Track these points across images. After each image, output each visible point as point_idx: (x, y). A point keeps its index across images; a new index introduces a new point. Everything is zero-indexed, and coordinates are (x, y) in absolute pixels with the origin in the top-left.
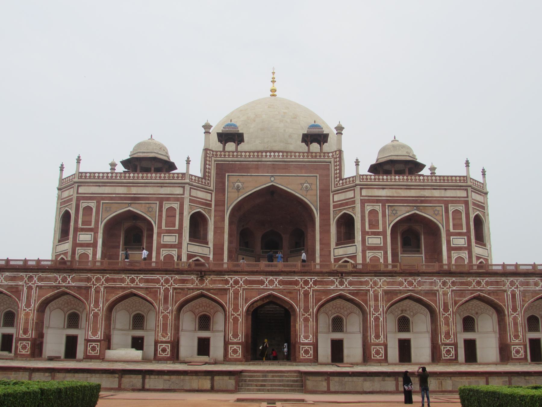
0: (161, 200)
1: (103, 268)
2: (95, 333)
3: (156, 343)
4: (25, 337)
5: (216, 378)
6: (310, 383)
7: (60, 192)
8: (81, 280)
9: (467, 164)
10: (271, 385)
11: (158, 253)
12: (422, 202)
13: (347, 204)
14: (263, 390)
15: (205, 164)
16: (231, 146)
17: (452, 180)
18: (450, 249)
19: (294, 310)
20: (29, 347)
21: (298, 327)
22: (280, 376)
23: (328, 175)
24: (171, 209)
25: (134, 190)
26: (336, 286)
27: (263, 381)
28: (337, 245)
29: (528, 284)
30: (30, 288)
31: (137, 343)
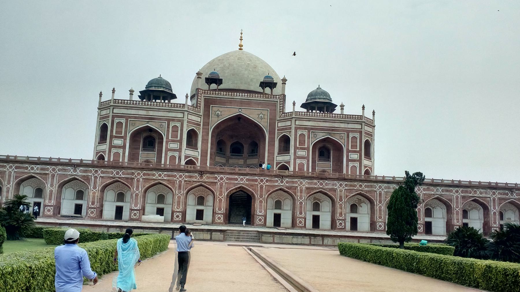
0: (169, 120)
1: (141, 167)
2: (136, 205)
3: (173, 213)
4: (93, 206)
5: (213, 233)
6: (264, 238)
7: (100, 110)
8: (128, 174)
9: (363, 107)
10: (243, 238)
12: (333, 130)
13: (286, 129)
14: (238, 241)
16: (214, 86)
17: (353, 117)
18: (348, 160)
19: (254, 196)
20: (95, 213)
21: (256, 206)
22: (247, 233)
24: (175, 127)
25: (151, 113)
26: (279, 183)
27: (238, 236)
29: (389, 188)
30: (96, 178)
31: (160, 211)
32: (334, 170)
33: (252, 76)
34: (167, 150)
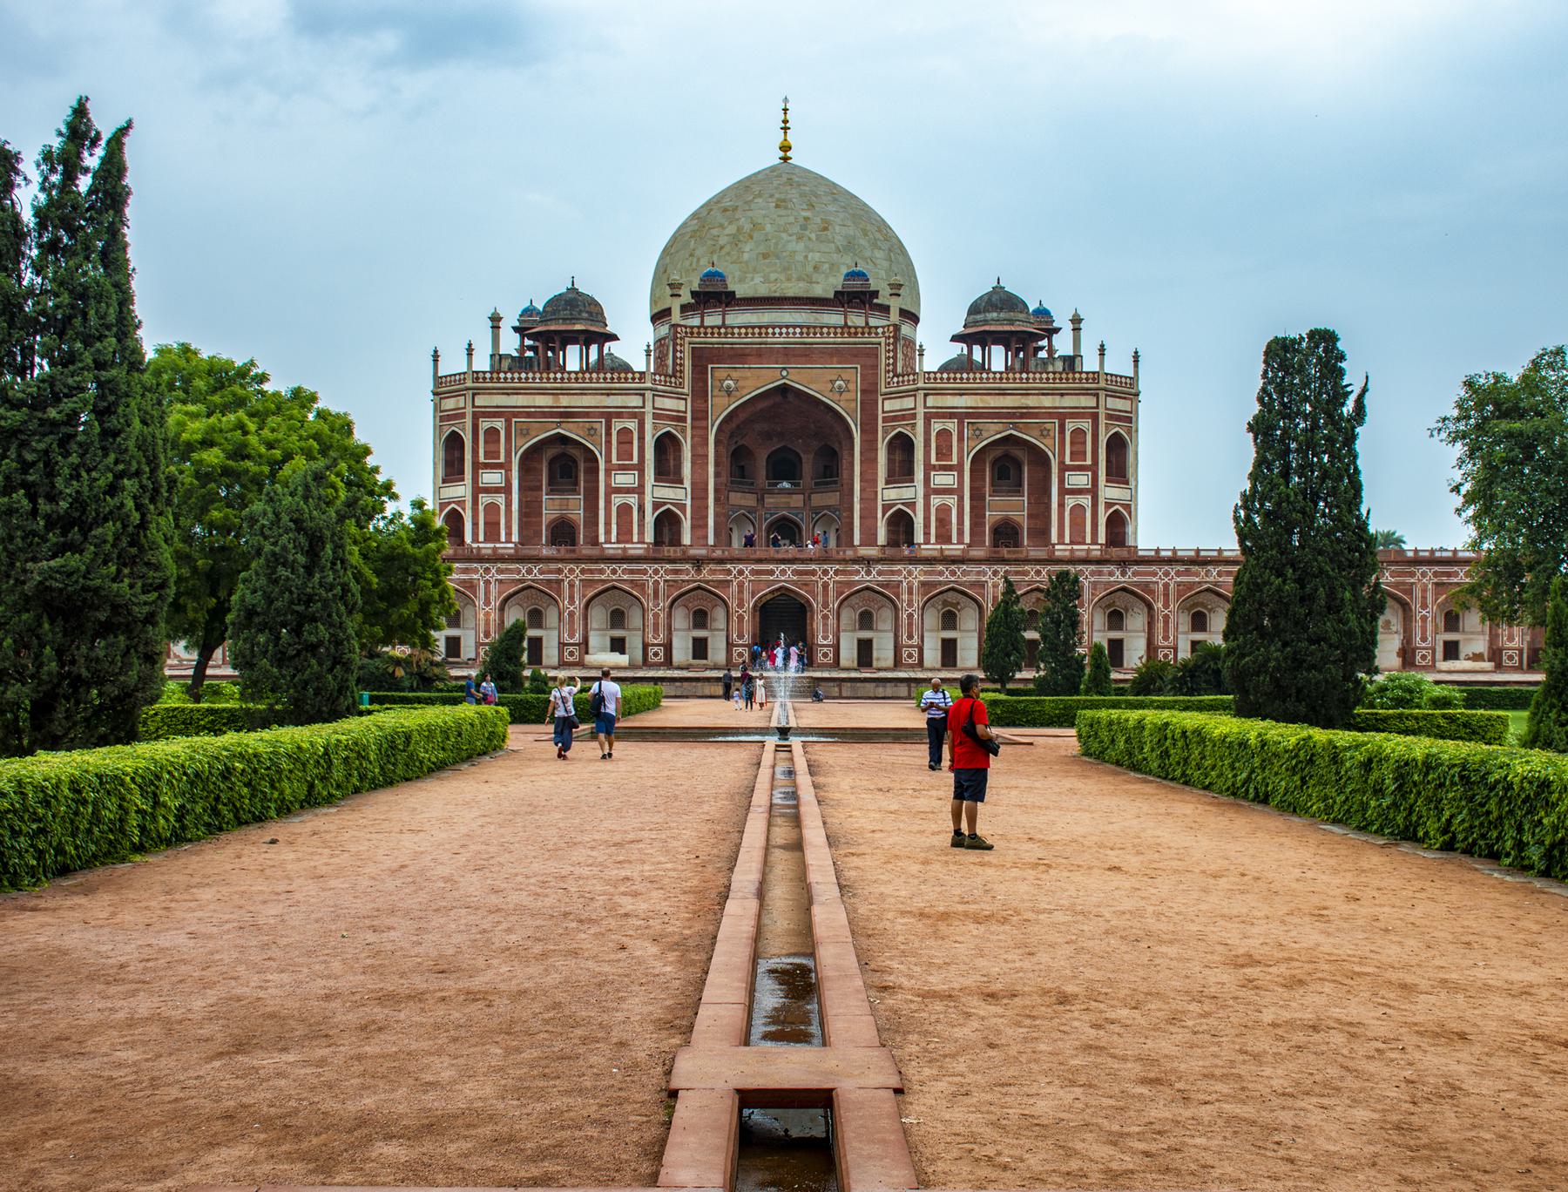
0: (609, 417)
2: (572, 636)
3: (645, 646)
8: (550, 572)
11: (608, 502)
12: (1023, 416)
13: (903, 418)
15: (675, 351)
18: (1063, 492)
19: (811, 605)
23: (875, 367)
24: (625, 432)
25: (565, 401)
26: (862, 577)
28: (887, 483)
29: (1100, 573)
30: (487, 583)
31: (618, 645)
32: (1030, 516)
33: (815, 257)
34: (611, 491)
